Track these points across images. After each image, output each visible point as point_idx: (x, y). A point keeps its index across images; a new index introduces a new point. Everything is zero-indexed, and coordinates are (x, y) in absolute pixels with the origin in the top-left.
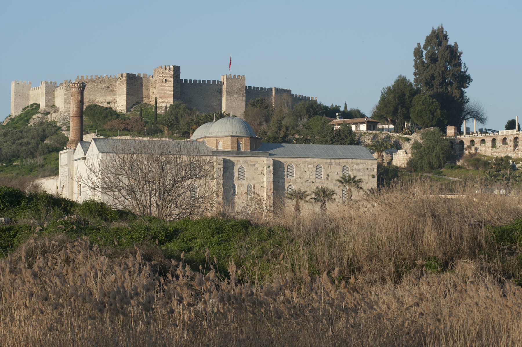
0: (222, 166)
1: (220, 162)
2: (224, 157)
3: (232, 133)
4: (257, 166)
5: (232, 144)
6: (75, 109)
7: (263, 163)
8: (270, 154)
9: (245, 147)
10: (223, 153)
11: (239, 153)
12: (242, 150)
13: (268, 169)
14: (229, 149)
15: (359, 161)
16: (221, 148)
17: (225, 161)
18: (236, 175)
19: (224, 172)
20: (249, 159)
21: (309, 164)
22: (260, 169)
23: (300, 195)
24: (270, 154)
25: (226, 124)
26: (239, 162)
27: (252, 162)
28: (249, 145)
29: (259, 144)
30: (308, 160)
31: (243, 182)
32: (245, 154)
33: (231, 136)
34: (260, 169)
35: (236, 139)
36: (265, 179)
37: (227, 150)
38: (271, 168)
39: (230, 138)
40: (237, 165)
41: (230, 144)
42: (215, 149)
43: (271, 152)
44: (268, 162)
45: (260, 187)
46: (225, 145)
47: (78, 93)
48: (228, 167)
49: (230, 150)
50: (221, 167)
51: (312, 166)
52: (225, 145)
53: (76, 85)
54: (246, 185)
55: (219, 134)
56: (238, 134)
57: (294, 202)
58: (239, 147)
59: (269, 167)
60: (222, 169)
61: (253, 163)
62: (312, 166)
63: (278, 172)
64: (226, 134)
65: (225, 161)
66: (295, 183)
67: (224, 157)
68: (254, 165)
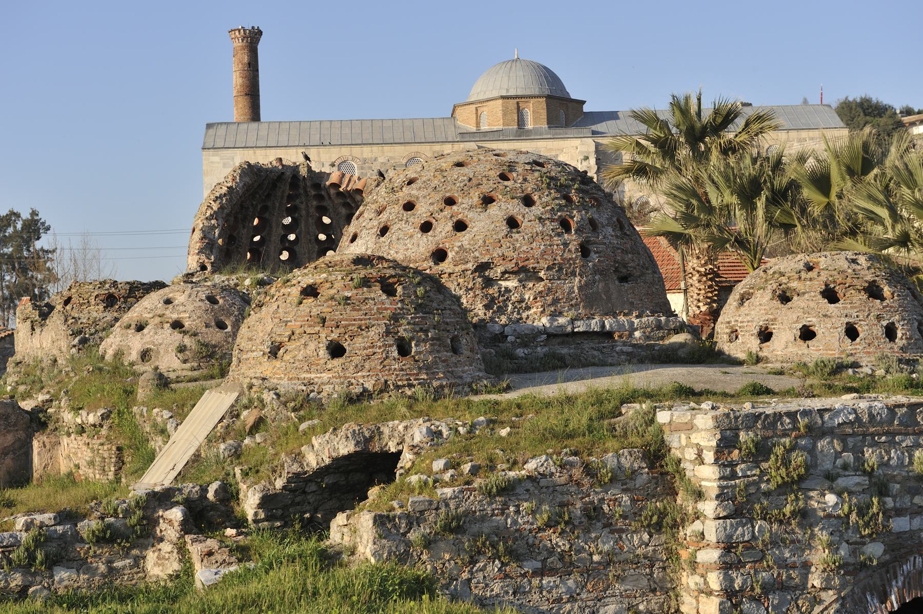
2: (480, 144)
3: (508, 90)
5: (504, 115)
8: (594, 133)
9: (535, 120)
12: (530, 126)
15: (804, 134)
16: (484, 127)
24: (594, 133)
25: (497, 73)
27: (551, 150)
32: (536, 134)
33: (503, 97)
37: (495, 128)
39: (500, 101)
41: (500, 114)
42: (474, 129)
44: (583, 149)
49: (501, 127)
55: (481, 97)
56: (520, 93)
58: (521, 122)
59: (586, 158)
64: (496, 94)
67: (480, 144)
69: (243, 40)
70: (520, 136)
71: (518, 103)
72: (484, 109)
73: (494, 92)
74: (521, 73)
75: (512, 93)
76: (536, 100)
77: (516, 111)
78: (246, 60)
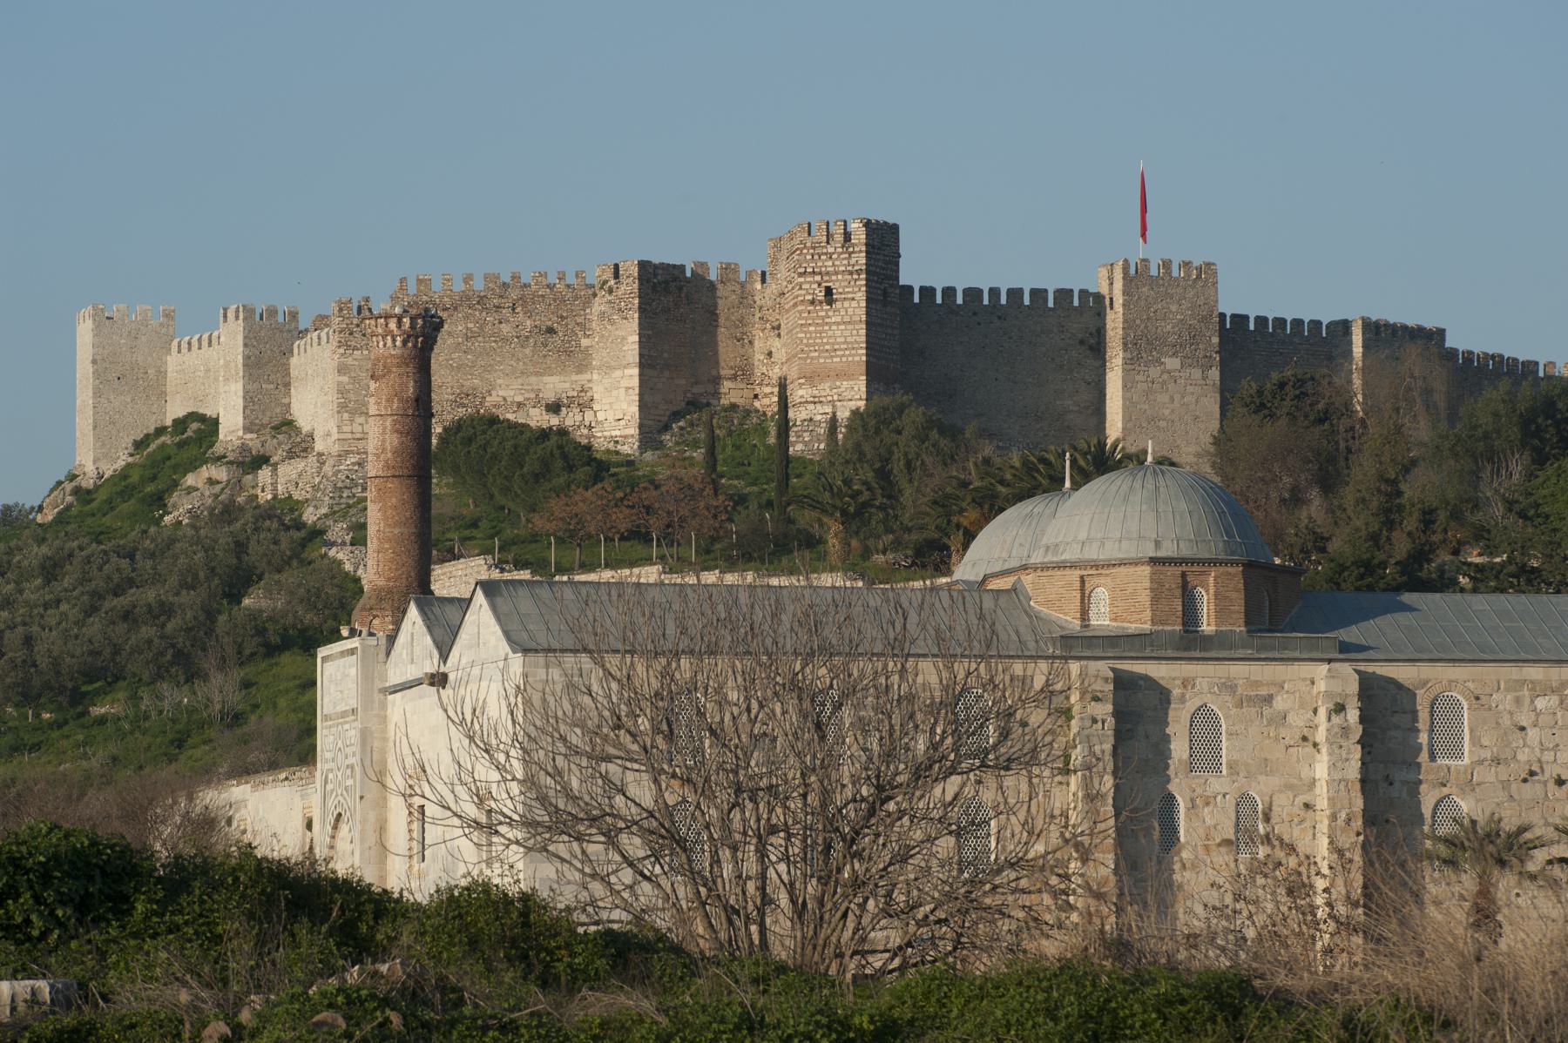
0: (1109, 708)
1: (1098, 686)
3: (1158, 544)
4: (1280, 703)
5: (1156, 599)
6: (393, 440)
7: (1311, 694)
8: (1345, 648)
9: (1221, 613)
10: (1115, 643)
11: (1189, 642)
12: (1207, 626)
13: (1336, 720)
14: (1141, 623)
16: (1102, 618)
17: (1124, 683)
18: (1179, 749)
19: (1121, 736)
20: (1239, 671)
21: (1540, 689)
22: (1297, 720)
23: (1497, 848)
25: (1126, 499)
26: (1193, 685)
28: (1239, 606)
29: (1288, 599)
30: (1535, 672)
31: (1216, 785)
33: (1154, 561)
34: (1297, 720)
35: (1176, 577)
36: (1321, 770)
37: (1133, 627)
38: (1353, 715)
39: (1146, 570)
40: (1182, 699)
41: (1145, 597)
42: (1075, 624)
43: (1351, 634)
44: (1337, 687)
45: (1297, 809)
46: (1121, 604)
47: (404, 362)
48: (1138, 713)
49: (1147, 627)
50: (1105, 710)
51: (1555, 700)
52: (1121, 604)
53: (393, 325)
54: (1231, 801)
55: (1092, 553)
56: (1186, 551)
57: (1468, 882)
59: (1340, 708)
60: (1111, 722)
61: (1264, 692)
62: (1555, 700)
63: (1387, 735)
64: (1129, 550)
65: (1124, 683)
66: (1469, 785)
68: (1269, 699)
69: (405, 343)
70: (1187, 649)
71: (1184, 575)
72: (1096, 580)
73: (1125, 544)
74: (1183, 506)
75: (1168, 550)
76: (1222, 569)
77: (1178, 592)
78: (411, 391)
